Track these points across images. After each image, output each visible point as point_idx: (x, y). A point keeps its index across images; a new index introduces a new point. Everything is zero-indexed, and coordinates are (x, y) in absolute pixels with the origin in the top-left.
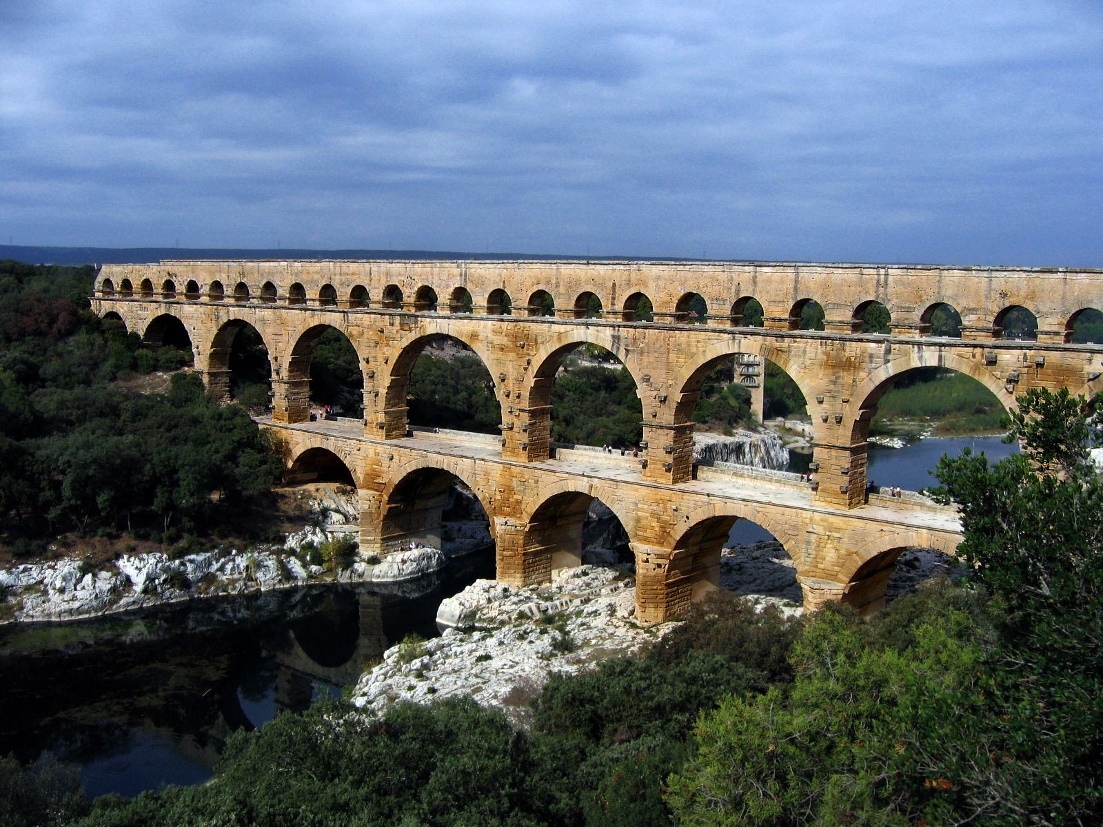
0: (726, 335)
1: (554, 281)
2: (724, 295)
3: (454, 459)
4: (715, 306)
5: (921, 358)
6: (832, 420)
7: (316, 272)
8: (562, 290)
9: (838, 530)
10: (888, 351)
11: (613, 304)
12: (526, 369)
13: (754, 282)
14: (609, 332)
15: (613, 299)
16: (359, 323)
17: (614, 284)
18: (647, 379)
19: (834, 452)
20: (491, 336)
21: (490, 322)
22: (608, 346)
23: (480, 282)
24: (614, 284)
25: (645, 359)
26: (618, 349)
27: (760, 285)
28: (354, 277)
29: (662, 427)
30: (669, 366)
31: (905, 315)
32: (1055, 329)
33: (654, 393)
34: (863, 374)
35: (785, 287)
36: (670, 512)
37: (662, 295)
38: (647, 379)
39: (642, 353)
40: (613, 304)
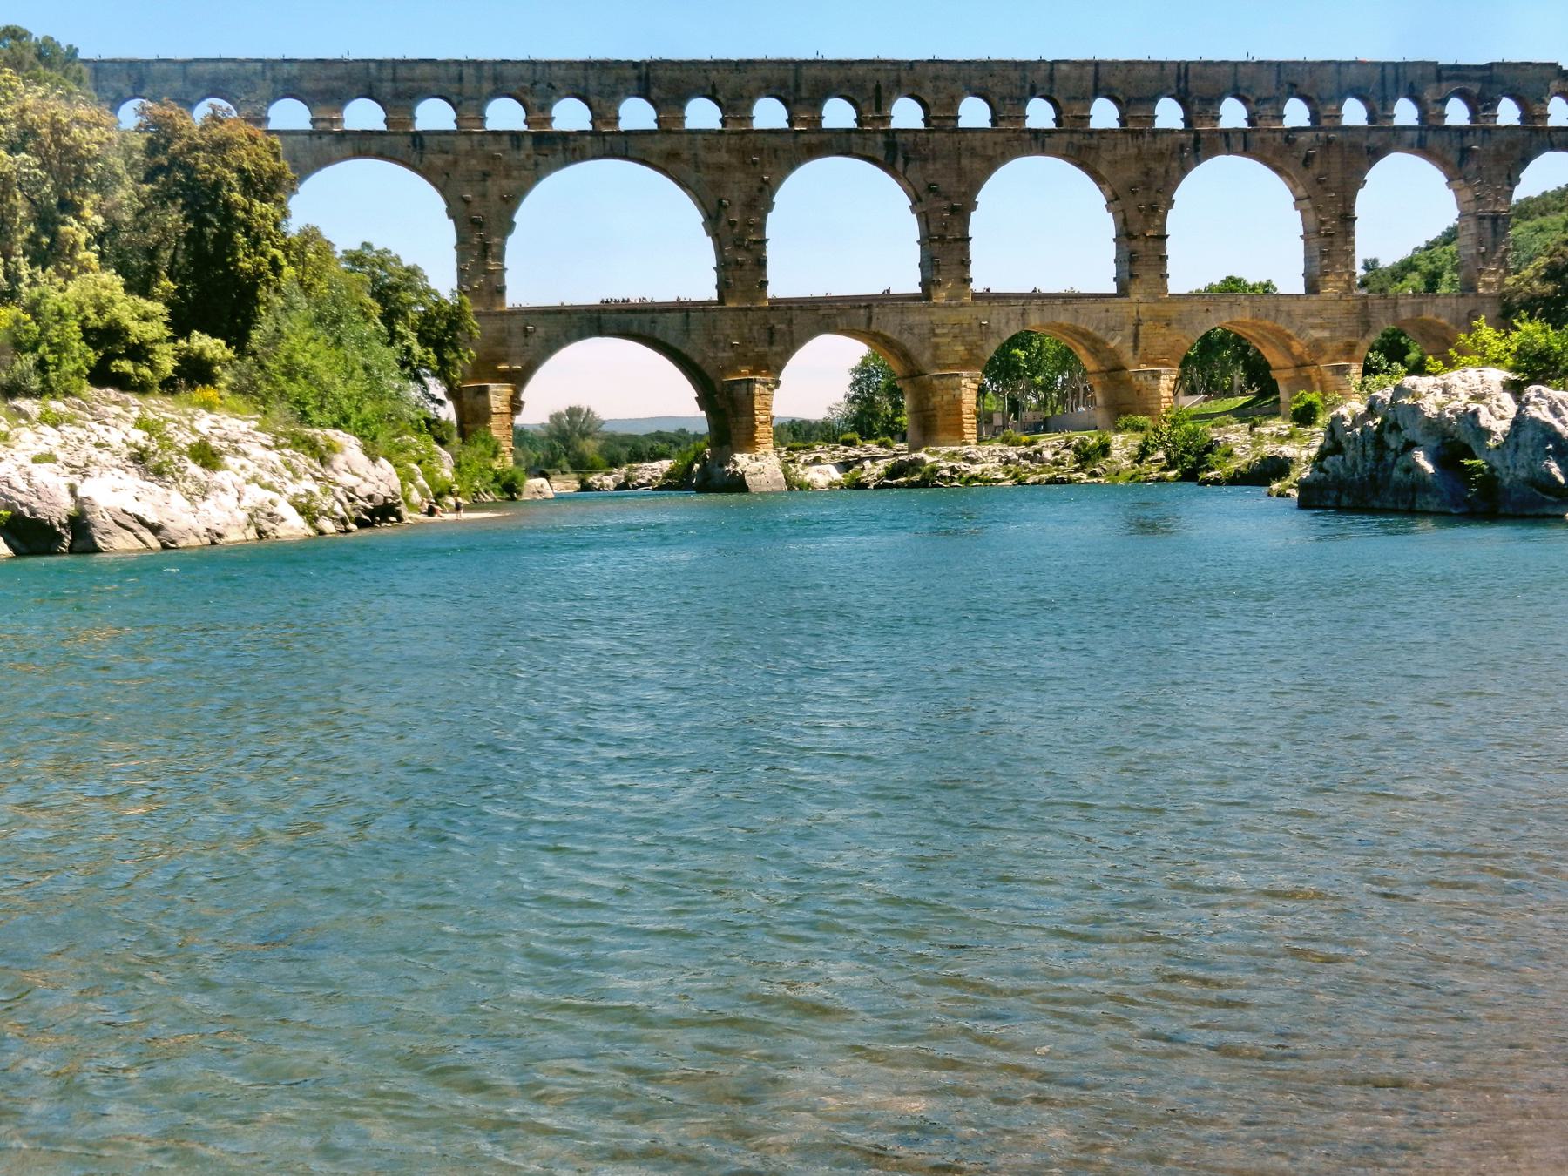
0: (1027, 136)
1: (791, 84)
2: (1017, 93)
3: (648, 317)
7: (336, 78)
8: (804, 93)
10: (1197, 140)
12: (761, 190)
13: (1051, 78)
16: (447, 147)
17: (878, 88)
18: (931, 189)
20: (702, 154)
24: (878, 88)
25: (930, 167)
26: (895, 158)
27: (1057, 81)
30: (960, 173)
34: (1174, 164)
37: (942, 96)
38: (931, 189)
39: (925, 159)
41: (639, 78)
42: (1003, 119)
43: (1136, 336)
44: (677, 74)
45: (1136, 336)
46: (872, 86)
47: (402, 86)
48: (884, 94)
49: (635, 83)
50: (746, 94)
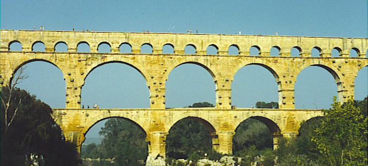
1: (174, 40)
4: (244, 49)
5: (313, 62)
6: (289, 82)
8: (179, 43)
9: (293, 115)
11: (202, 48)
12: (164, 73)
13: (257, 41)
14: (202, 57)
15: (202, 46)
19: (289, 92)
21: (144, 56)
22: (202, 63)
23: (137, 41)
25: (219, 67)
26: (207, 64)
28: (57, 38)
29: (226, 90)
31: (307, 50)
32: (347, 53)
33: (223, 78)
35: (268, 43)
36: (233, 118)
39: (217, 65)
40: (202, 48)
41: (126, 38)
42: (242, 52)
43: (284, 121)
44: (138, 37)
45: (284, 121)
46: (201, 41)
47: (50, 39)
48: (204, 44)
49: (125, 39)
50: (160, 43)
